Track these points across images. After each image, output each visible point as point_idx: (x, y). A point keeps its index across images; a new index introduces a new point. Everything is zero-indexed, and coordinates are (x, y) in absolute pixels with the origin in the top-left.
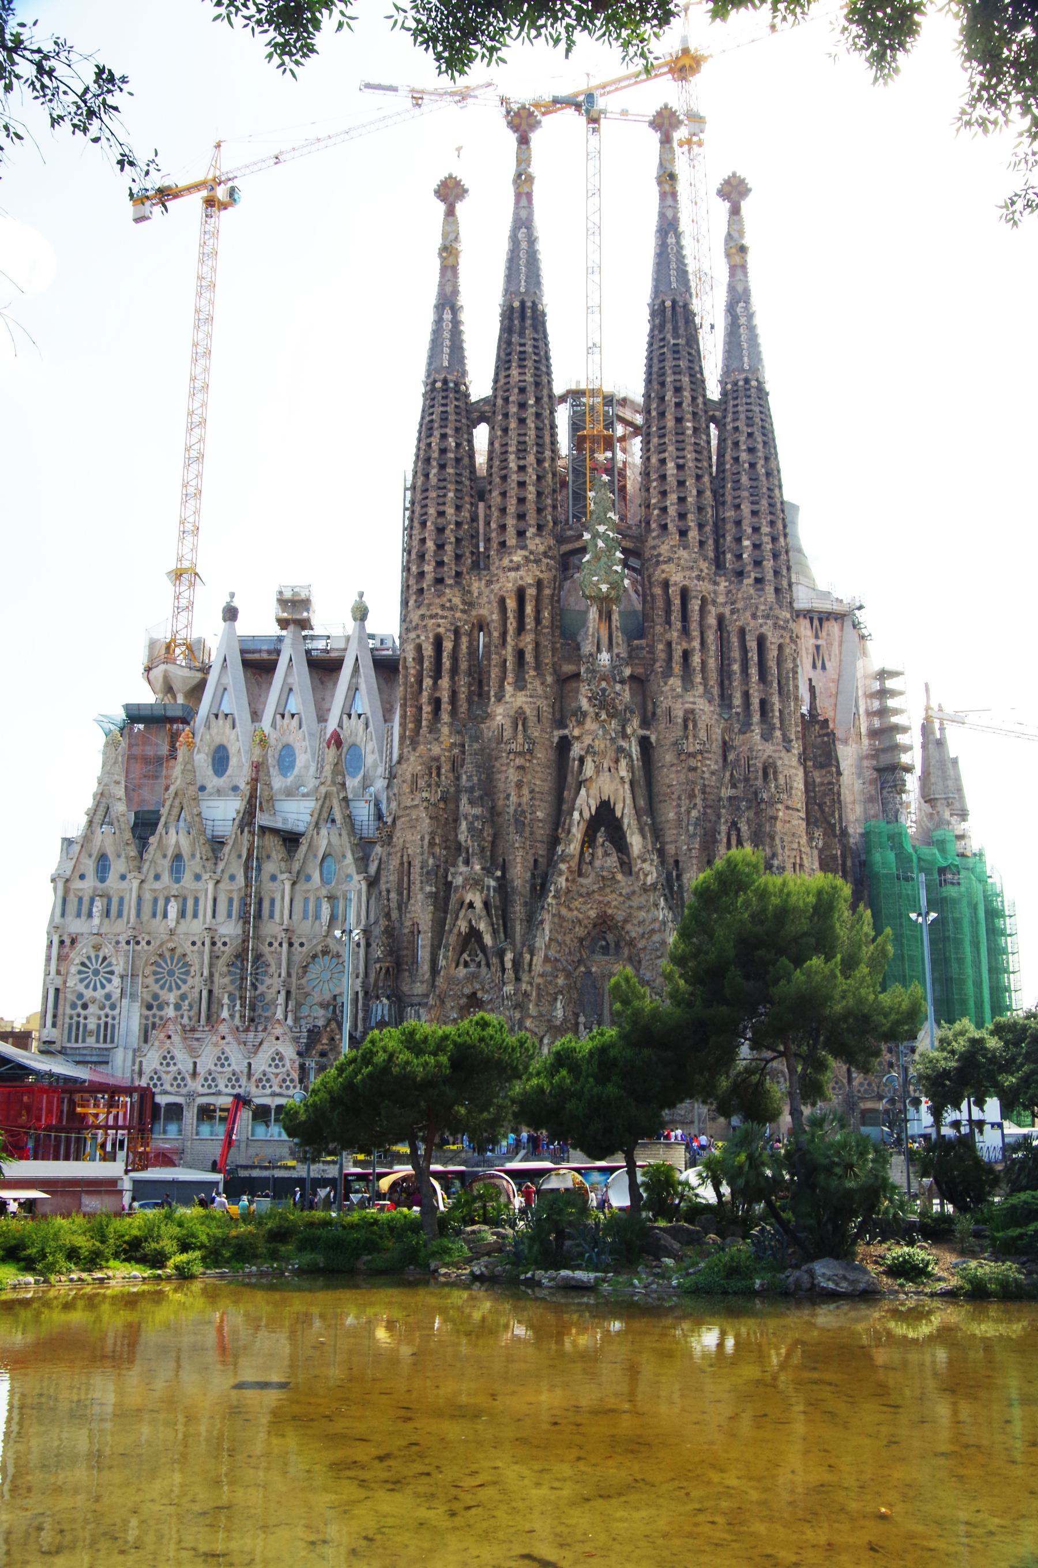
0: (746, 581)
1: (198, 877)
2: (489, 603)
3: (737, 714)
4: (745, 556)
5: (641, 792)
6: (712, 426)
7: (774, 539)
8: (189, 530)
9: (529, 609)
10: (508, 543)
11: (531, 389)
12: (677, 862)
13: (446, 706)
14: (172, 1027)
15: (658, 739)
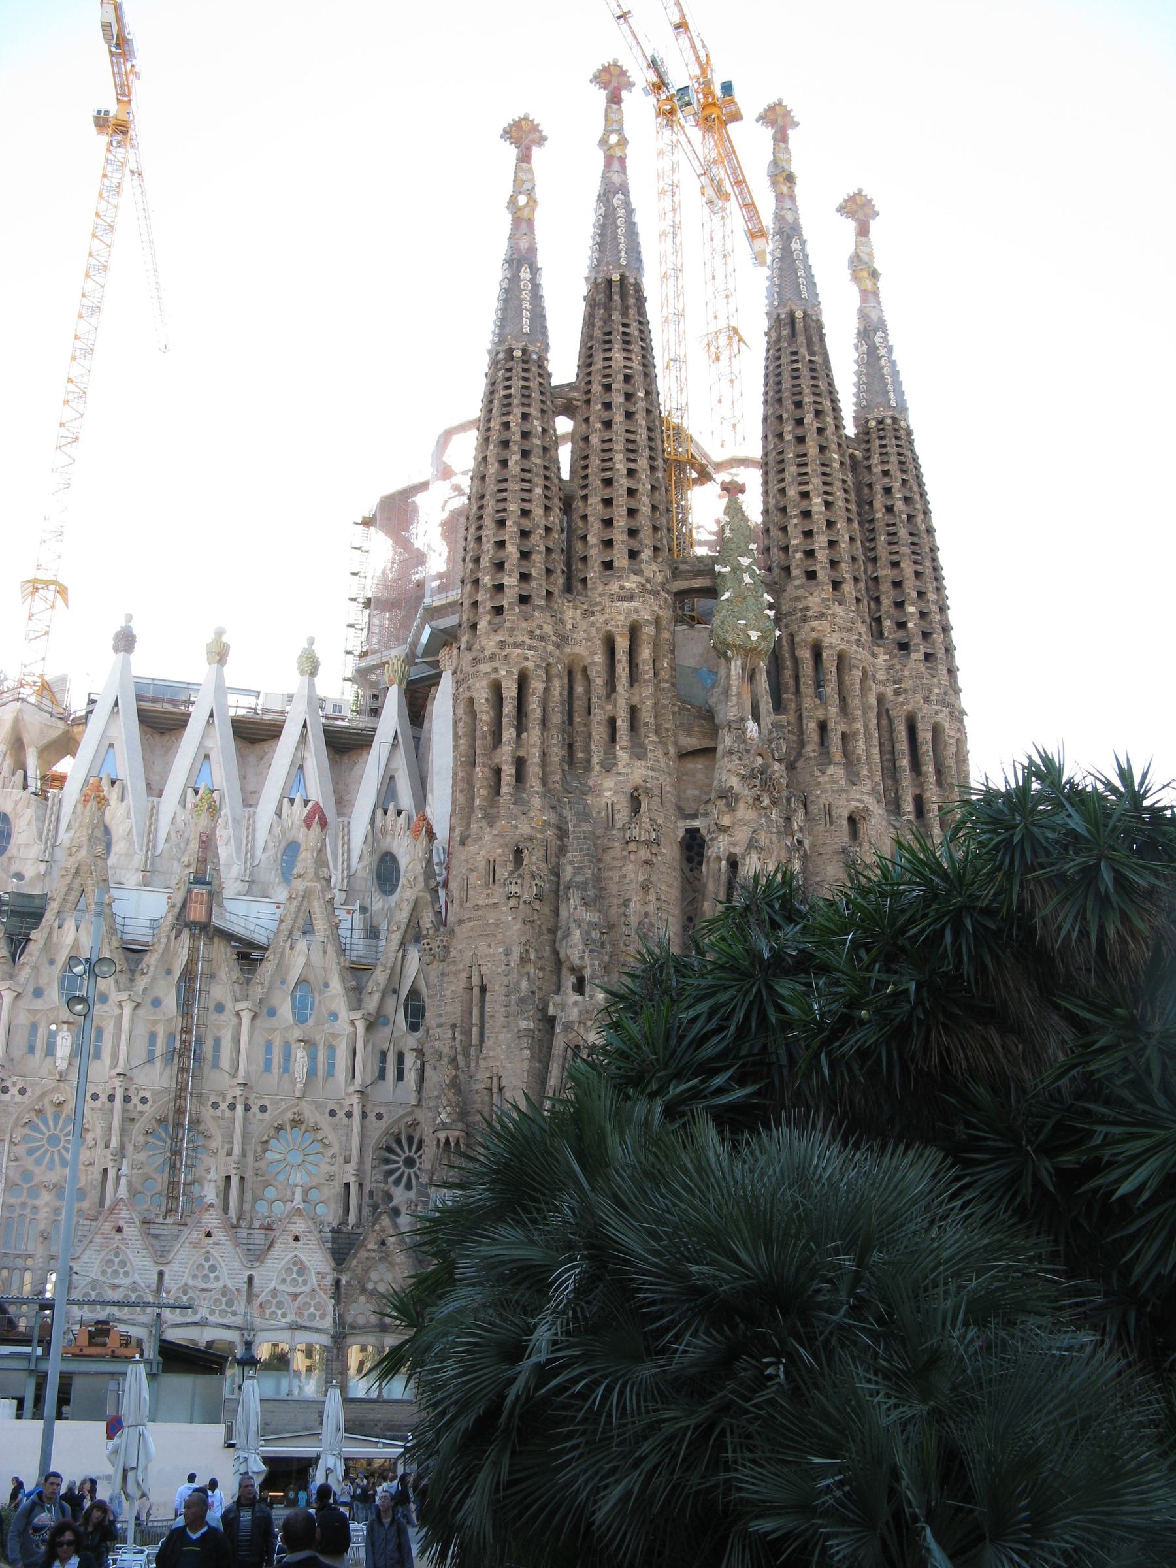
0: (914, 656)
2: (586, 639)
4: (910, 625)
9: (645, 653)
10: (616, 564)
11: (639, 379)
13: (533, 769)
14: (124, 1214)
15: (813, 846)
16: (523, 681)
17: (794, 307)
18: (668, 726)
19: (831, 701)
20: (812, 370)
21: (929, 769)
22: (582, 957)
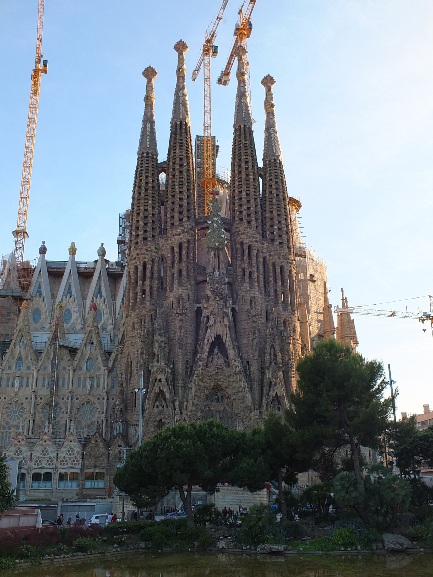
0: (275, 243)
1: (29, 368)
2: (166, 249)
3: (272, 298)
4: (275, 233)
5: (233, 331)
6: (260, 178)
7: (287, 226)
8: (23, 214)
9: (184, 252)
10: (175, 224)
11: (185, 159)
12: (248, 362)
13: (148, 293)
14: (21, 437)
15: (239, 309)
16: (145, 265)
17: (241, 124)
18: (192, 275)
19: (245, 262)
20: (245, 147)
21: (279, 281)
22: (158, 352)
